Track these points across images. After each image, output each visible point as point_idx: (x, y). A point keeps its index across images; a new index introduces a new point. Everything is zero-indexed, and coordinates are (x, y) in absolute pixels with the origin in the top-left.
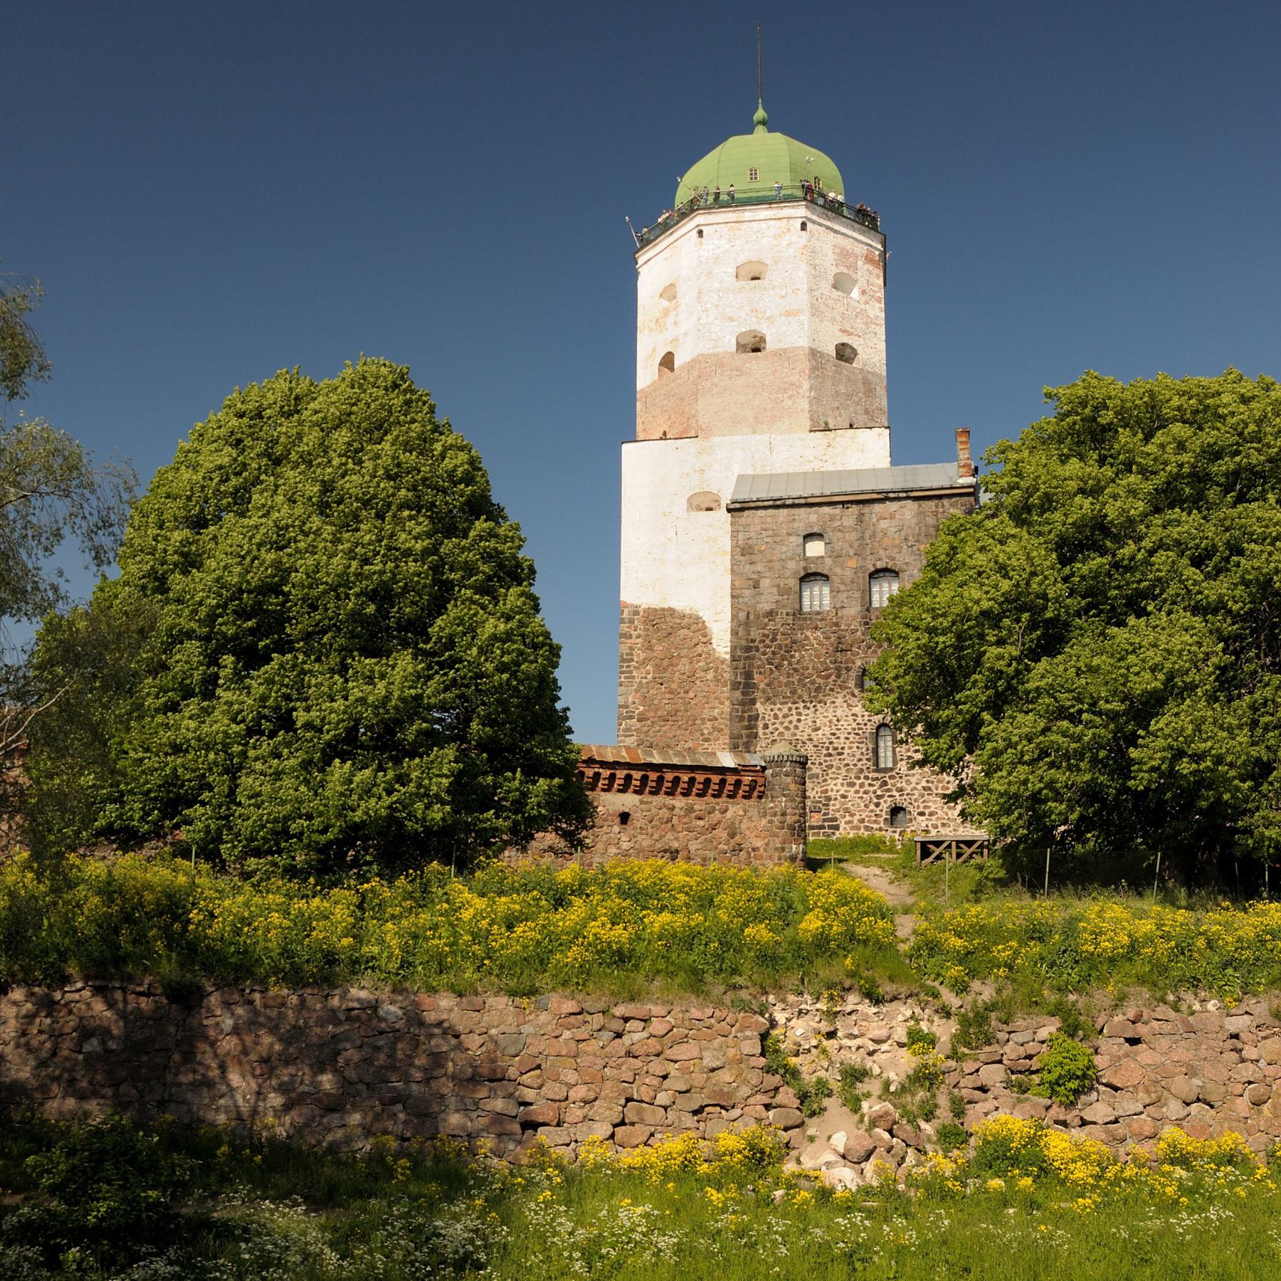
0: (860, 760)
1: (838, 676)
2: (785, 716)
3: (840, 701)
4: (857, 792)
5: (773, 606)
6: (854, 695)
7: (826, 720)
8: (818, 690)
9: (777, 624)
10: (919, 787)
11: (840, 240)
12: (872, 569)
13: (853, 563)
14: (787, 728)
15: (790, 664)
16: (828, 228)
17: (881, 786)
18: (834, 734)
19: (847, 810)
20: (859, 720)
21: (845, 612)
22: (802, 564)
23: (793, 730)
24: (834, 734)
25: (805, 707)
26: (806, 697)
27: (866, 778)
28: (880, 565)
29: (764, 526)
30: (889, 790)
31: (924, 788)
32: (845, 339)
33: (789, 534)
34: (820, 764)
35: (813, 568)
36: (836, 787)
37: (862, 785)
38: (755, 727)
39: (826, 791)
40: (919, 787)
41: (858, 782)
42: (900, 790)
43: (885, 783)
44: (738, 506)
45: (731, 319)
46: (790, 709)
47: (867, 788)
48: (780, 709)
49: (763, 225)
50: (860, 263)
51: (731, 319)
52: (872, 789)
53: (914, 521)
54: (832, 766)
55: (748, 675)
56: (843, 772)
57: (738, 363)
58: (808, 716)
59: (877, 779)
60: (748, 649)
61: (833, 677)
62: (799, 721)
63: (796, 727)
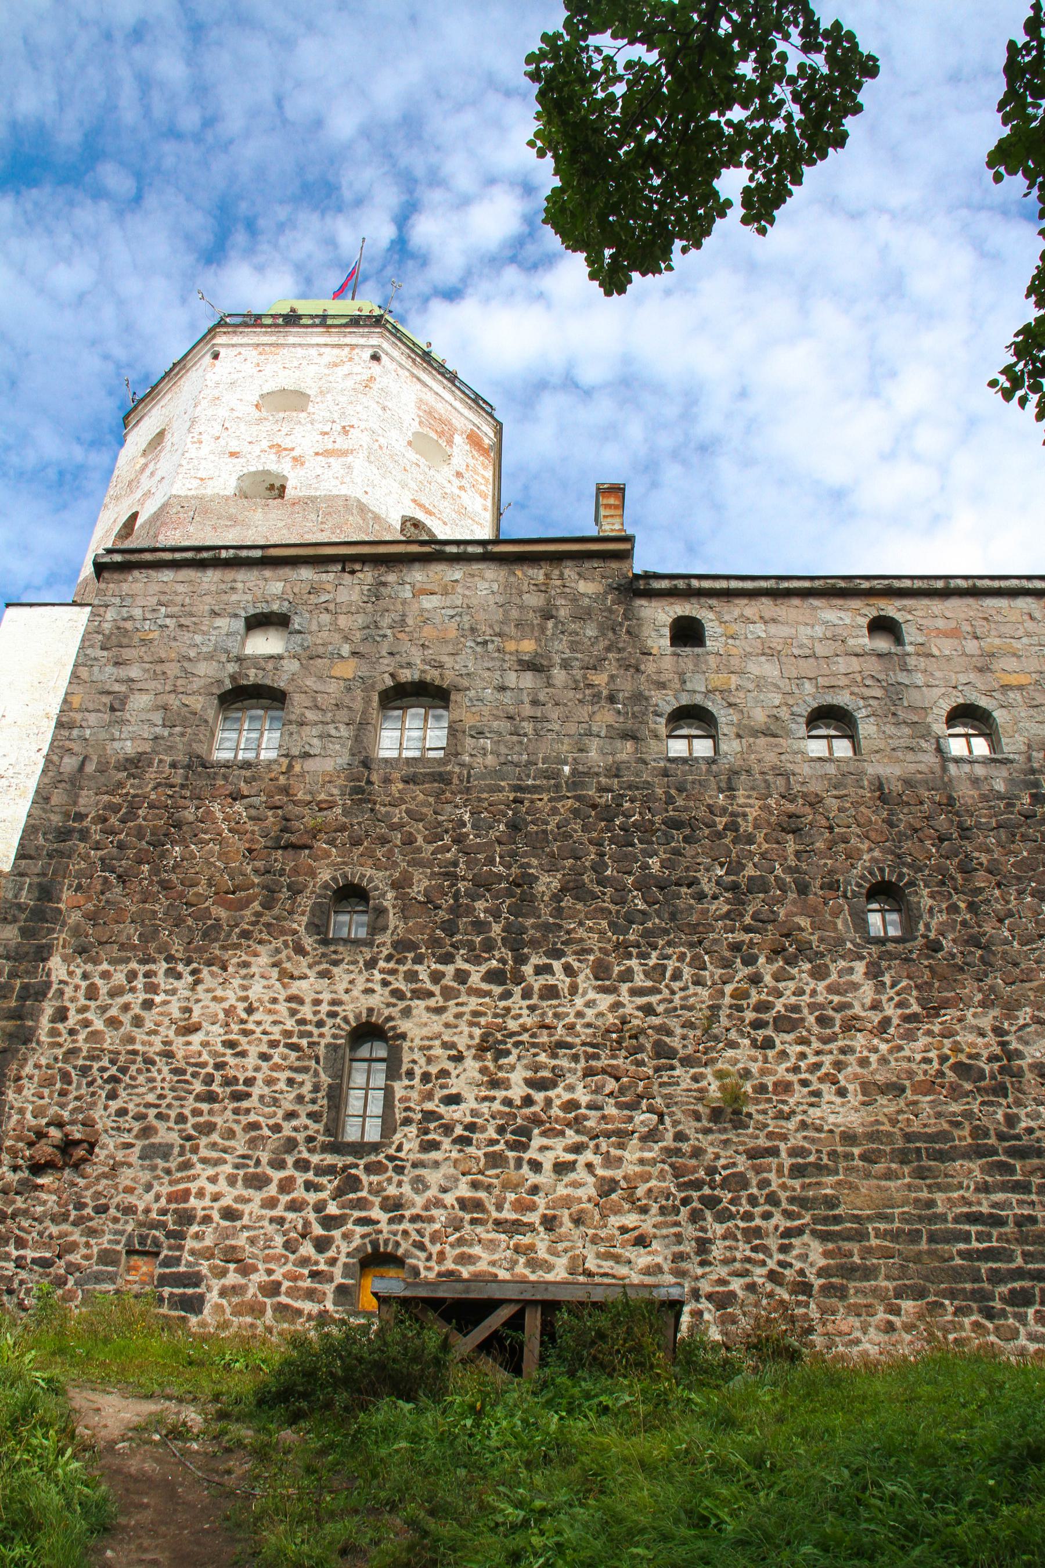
0: (291, 1115)
1: (267, 905)
2: (115, 992)
3: (262, 961)
4: (270, 1203)
5: (147, 747)
6: (300, 950)
7: (217, 1008)
8: (211, 933)
9: (148, 785)
10: (449, 1199)
11: (430, 398)
13: (348, 669)
14: (113, 1023)
15: (155, 871)
16: (413, 375)
18: (231, 1044)
19: (232, 1255)
20: (306, 1011)
21: (310, 765)
22: (232, 668)
23: (127, 1028)
24: (231, 1044)
25: (173, 973)
26: (177, 949)
27: (302, 1165)
28: (406, 675)
29: (164, 599)
30: (361, 1204)
31: (463, 1204)
32: (420, 516)
33: (215, 614)
34: (181, 1119)
35: (253, 676)
36: (212, 1186)
37: (285, 1186)
38: (35, 1015)
39: (186, 1195)
40: (449, 1199)
41: (277, 1175)
42: (394, 1205)
43: (354, 1184)
44: (118, 558)
45: (233, 454)
46: (132, 976)
47: (299, 1193)
48: (106, 975)
49: (313, 351)
50: (458, 439)
51: (233, 454)
52: (312, 1197)
54: (210, 1127)
55: (46, 892)
56: (240, 1145)
57: (233, 511)
58: (174, 995)
59: (331, 1170)
60: (63, 834)
61: (256, 906)
62: (148, 1005)
63: (138, 1022)
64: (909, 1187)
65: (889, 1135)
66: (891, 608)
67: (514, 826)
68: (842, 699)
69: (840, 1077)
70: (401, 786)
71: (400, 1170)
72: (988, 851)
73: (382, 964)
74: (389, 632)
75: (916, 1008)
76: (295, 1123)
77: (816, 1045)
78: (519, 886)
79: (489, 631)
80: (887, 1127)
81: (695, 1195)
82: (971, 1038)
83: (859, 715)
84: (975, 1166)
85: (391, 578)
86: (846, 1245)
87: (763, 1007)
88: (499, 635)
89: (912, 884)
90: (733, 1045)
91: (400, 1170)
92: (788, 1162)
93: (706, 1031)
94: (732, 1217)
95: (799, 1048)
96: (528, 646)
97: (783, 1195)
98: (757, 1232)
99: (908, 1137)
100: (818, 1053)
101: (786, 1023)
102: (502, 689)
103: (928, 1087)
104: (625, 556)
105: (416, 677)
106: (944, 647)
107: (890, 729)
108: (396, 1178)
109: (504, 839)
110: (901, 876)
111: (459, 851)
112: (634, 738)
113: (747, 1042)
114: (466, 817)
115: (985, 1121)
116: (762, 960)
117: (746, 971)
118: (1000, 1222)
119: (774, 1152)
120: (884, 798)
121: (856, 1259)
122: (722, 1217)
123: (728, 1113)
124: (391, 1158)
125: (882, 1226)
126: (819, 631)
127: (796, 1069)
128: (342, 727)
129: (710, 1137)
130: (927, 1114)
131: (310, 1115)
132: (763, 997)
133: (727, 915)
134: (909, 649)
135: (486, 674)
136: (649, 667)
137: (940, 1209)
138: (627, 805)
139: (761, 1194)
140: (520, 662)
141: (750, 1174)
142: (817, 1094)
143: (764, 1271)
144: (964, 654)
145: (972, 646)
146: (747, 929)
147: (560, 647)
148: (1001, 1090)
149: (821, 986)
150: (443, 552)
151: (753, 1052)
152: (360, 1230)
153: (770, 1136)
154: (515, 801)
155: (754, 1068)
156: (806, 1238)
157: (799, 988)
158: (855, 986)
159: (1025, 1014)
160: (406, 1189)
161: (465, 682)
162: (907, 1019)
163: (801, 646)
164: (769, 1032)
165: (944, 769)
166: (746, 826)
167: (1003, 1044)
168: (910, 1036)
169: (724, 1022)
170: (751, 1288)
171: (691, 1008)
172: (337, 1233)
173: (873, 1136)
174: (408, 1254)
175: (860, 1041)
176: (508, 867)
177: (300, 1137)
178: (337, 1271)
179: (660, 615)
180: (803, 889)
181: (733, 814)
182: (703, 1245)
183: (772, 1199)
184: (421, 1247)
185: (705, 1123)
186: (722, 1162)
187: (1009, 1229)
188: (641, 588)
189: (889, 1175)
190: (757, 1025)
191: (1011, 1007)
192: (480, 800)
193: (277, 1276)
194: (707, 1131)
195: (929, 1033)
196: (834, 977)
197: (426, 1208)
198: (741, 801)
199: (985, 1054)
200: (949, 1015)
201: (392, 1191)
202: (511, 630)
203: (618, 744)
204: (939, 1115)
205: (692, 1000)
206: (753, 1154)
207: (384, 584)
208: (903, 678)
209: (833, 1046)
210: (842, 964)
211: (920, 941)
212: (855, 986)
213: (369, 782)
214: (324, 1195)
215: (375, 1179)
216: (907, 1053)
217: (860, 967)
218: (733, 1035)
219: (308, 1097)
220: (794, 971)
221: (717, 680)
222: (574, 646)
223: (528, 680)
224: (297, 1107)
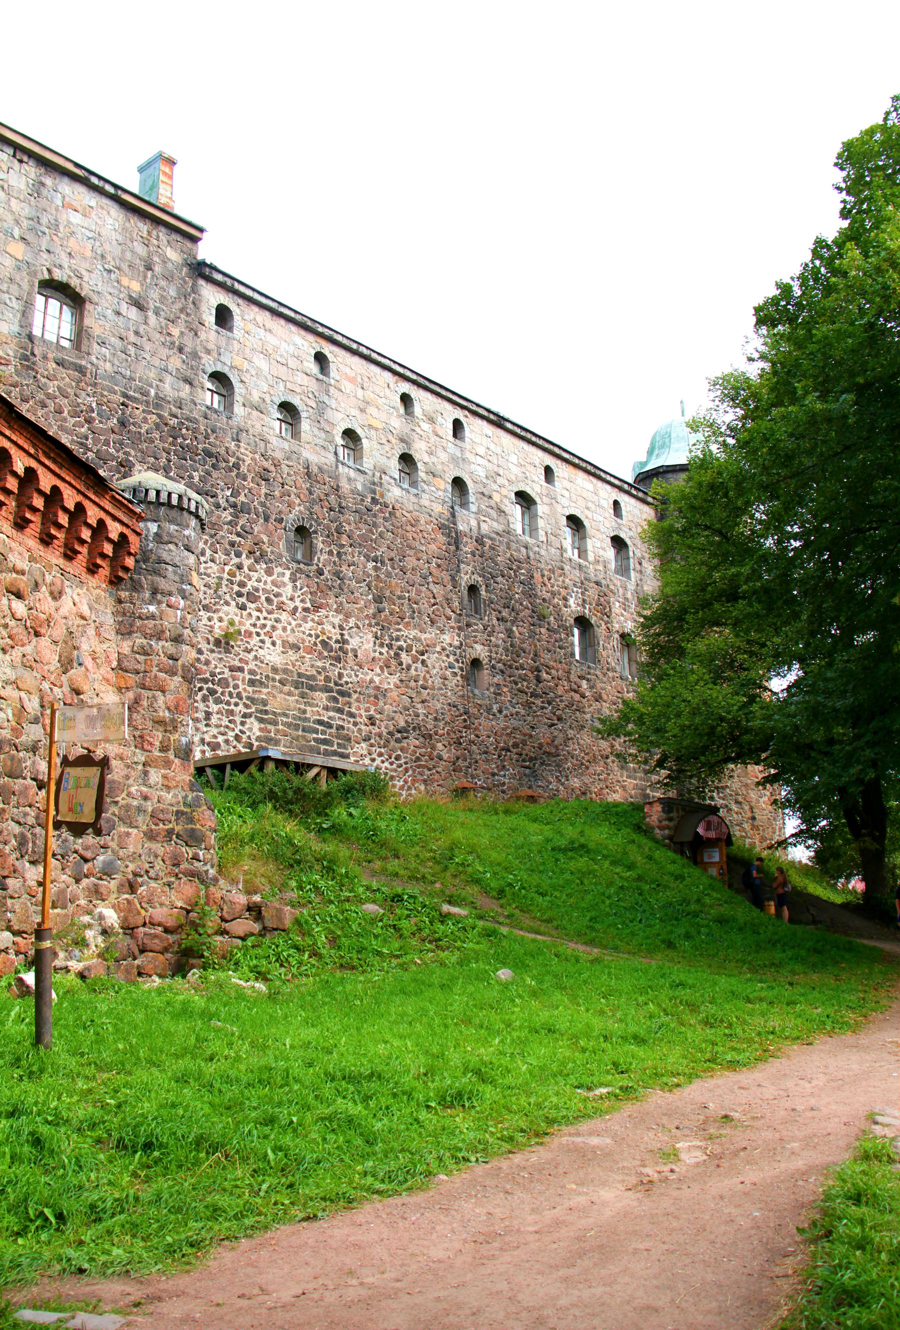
12: (47, 276)
28: (58, 275)
53: (114, 236)
64: (297, 701)
65: (292, 672)
66: (328, 350)
67: (123, 423)
68: (296, 401)
69: (274, 634)
70: (54, 365)
72: (349, 524)
74: (47, 231)
75: (308, 605)
77: (265, 614)
78: (123, 466)
79: (112, 263)
80: (290, 667)
81: (205, 686)
82: (330, 628)
83: (304, 415)
84: (324, 695)
85: (48, 181)
86: (269, 727)
87: (242, 584)
88: (119, 269)
89: (315, 532)
90: (227, 603)
92: (248, 677)
93: (216, 592)
94: (221, 702)
95: (258, 614)
96: (136, 287)
97: (244, 695)
98: (231, 713)
99: (300, 675)
100: (265, 618)
101: (252, 597)
102: (118, 313)
103: (310, 651)
104: (195, 240)
105: (65, 280)
106: (347, 386)
107: (316, 431)
109: (116, 430)
110: (311, 525)
111: (89, 429)
112: (191, 384)
113: (233, 603)
114: (94, 405)
115: (330, 674)
116: (244, 556)
117: (236, 560)
118: (330, 726)
119: (241, 670)
120: (308, 474)
121: (272, 734)
122: (218, 701)
123: (224, 643)
125: (285, 719)
126: (291, 349)
127: (255, 625)
128: (14, 300)
129: (214, 655)
130: (309, 664)
133: (230, 523)
134: (332, 382)
135: (109, 297)
136: (203, 335)
137: (308, 716)
138: (184, 431)
139: (235, 692)
140: (130, 297)
141: (230, 680)
142: (262, 641)
143: (233, 734)
144: (355, 396)
145: (360, 393)
146: (238, 535)
147: (154, 294)
148: (338, 659)
149: (269, 579)
150: (89, 180)
151: (236, 610)
153: (241, 660)
154: (123, 404)
155: (237, 619)
156: (252, 719)
157: (258, 579)
158: (284, 585)
159: (352, 621)
161: (95, 298)
162: (305, 610)
163: (281, 356)
164: (243, 600)
165: (337, 467)
166: (244, 469)
167: (342, 635)
168: (305, 619)
169: (224, 589)
170: (227, 742)
171: (209, 576)
173: (285, 671)
175: (284, 616)
176: (118, 451)
179: (212, 297)
180: (267, 519)
181: (238, 458)
182: (208, 715)
183: (239, 696)
185: (211, 646)
186: (218, 670)
187: (334, 730)
188: (201, 271)
189: (289, 694)
190: (240, 595)
191: (348, 616)
192: (102, 395)
194: (212, 651)
195: (313, 620)
196: (275, 576)
198: (243, 450)
199: (334, 638)
200: (323, 612)
202: (125, 267)
203: (182, 384)
204: (312, 666)
205: (209, 571)
206: (232, 669)
207: (43, 184)
208: (326, 399)
209: (272, 616)
210: (280, 570)
211: (315, 567)
212: (284, 585)
213: (33, 354)
216: (302, 629)
217: (288, 573)
218: (228, 597)
221: (238, 361)
222: (163, 299)
223: (133, 313)
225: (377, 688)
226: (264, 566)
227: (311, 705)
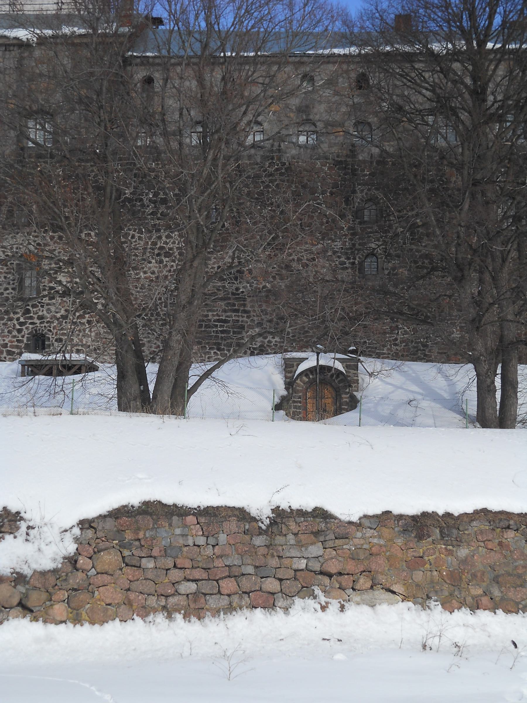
17: (24, 314)
42: (41, 318)
43: (28, 311)
71: (42, 306)
73: (33, 234)
76: (8, 292)
84: (222, 303)
87: (161, 248)
90: (150, 262)
91: (42, 306)
108: (42, 309)
124: (39, 303)
131: (13, 289)
132: (162, 245)
133: (152, 214)
152: (31, 326)
160: (45, 312)
172: (24, 328)
174: (46, 333)
177: (10, 296)
178: (25, 340)
184: (50, 331)
190: (158, 255)
193: (6, 342)
195: (215, 258)
197: (51, 319)
201: (40, 313)
214: (19, 316)
215: (35, 309)
219: (11, 282)
220: (173, 235)
224: (8, 286)
225: (269, 291)
226: (176, 233)
227: (214, 311)
